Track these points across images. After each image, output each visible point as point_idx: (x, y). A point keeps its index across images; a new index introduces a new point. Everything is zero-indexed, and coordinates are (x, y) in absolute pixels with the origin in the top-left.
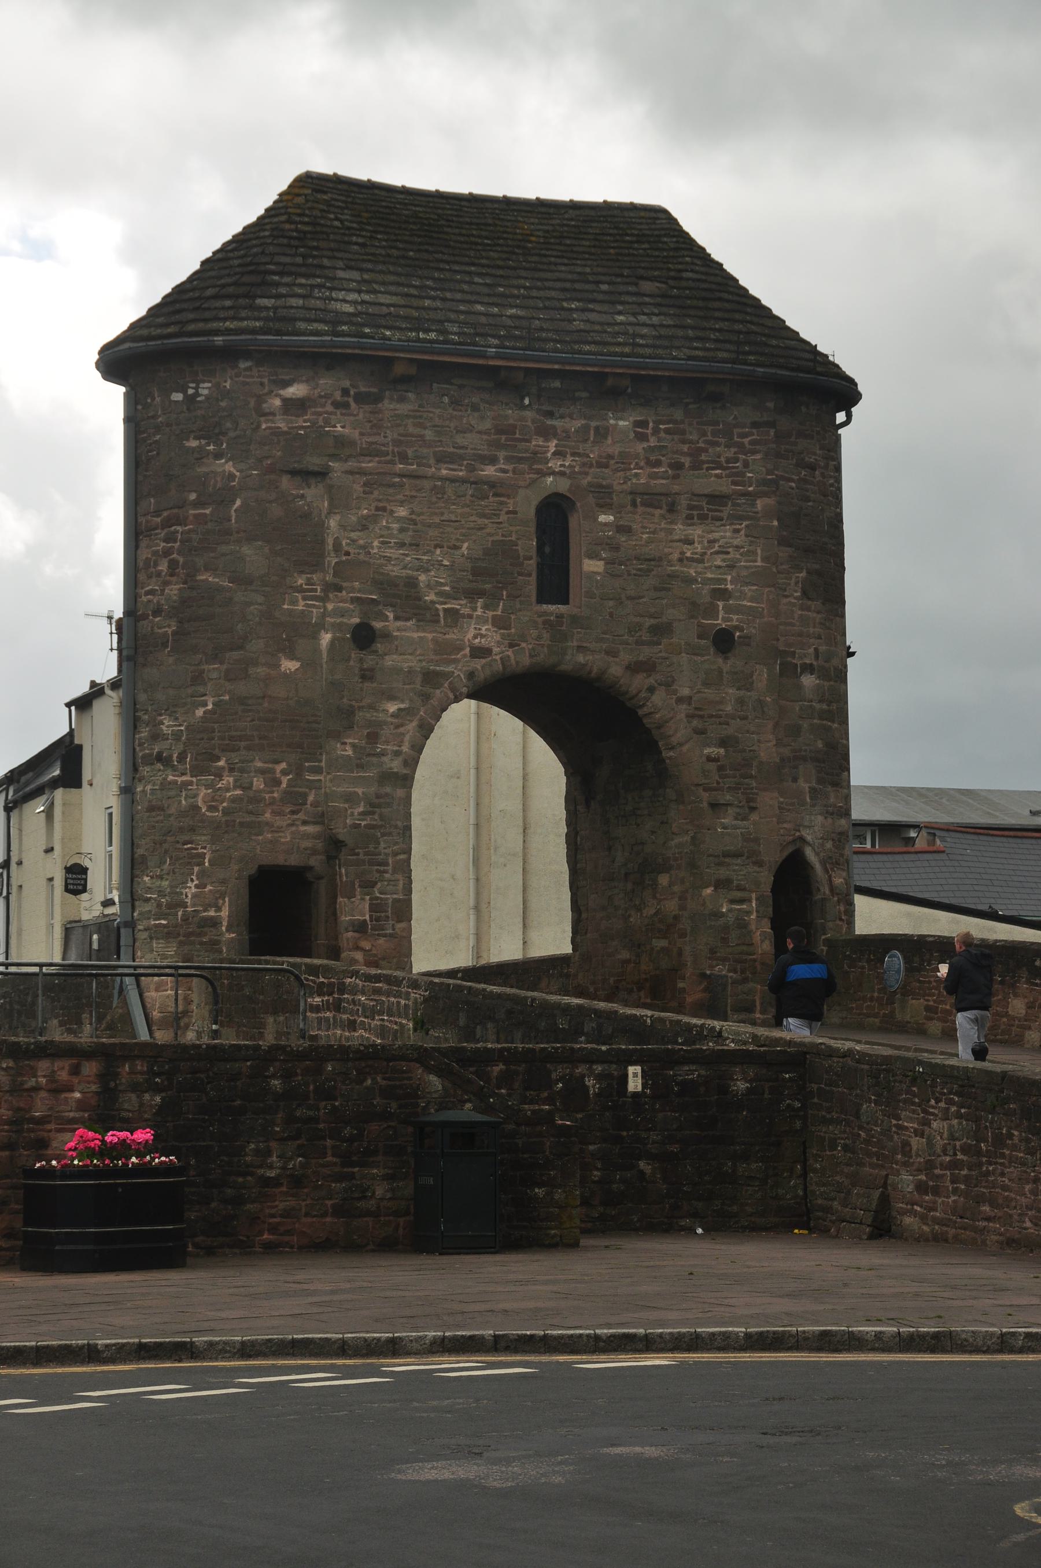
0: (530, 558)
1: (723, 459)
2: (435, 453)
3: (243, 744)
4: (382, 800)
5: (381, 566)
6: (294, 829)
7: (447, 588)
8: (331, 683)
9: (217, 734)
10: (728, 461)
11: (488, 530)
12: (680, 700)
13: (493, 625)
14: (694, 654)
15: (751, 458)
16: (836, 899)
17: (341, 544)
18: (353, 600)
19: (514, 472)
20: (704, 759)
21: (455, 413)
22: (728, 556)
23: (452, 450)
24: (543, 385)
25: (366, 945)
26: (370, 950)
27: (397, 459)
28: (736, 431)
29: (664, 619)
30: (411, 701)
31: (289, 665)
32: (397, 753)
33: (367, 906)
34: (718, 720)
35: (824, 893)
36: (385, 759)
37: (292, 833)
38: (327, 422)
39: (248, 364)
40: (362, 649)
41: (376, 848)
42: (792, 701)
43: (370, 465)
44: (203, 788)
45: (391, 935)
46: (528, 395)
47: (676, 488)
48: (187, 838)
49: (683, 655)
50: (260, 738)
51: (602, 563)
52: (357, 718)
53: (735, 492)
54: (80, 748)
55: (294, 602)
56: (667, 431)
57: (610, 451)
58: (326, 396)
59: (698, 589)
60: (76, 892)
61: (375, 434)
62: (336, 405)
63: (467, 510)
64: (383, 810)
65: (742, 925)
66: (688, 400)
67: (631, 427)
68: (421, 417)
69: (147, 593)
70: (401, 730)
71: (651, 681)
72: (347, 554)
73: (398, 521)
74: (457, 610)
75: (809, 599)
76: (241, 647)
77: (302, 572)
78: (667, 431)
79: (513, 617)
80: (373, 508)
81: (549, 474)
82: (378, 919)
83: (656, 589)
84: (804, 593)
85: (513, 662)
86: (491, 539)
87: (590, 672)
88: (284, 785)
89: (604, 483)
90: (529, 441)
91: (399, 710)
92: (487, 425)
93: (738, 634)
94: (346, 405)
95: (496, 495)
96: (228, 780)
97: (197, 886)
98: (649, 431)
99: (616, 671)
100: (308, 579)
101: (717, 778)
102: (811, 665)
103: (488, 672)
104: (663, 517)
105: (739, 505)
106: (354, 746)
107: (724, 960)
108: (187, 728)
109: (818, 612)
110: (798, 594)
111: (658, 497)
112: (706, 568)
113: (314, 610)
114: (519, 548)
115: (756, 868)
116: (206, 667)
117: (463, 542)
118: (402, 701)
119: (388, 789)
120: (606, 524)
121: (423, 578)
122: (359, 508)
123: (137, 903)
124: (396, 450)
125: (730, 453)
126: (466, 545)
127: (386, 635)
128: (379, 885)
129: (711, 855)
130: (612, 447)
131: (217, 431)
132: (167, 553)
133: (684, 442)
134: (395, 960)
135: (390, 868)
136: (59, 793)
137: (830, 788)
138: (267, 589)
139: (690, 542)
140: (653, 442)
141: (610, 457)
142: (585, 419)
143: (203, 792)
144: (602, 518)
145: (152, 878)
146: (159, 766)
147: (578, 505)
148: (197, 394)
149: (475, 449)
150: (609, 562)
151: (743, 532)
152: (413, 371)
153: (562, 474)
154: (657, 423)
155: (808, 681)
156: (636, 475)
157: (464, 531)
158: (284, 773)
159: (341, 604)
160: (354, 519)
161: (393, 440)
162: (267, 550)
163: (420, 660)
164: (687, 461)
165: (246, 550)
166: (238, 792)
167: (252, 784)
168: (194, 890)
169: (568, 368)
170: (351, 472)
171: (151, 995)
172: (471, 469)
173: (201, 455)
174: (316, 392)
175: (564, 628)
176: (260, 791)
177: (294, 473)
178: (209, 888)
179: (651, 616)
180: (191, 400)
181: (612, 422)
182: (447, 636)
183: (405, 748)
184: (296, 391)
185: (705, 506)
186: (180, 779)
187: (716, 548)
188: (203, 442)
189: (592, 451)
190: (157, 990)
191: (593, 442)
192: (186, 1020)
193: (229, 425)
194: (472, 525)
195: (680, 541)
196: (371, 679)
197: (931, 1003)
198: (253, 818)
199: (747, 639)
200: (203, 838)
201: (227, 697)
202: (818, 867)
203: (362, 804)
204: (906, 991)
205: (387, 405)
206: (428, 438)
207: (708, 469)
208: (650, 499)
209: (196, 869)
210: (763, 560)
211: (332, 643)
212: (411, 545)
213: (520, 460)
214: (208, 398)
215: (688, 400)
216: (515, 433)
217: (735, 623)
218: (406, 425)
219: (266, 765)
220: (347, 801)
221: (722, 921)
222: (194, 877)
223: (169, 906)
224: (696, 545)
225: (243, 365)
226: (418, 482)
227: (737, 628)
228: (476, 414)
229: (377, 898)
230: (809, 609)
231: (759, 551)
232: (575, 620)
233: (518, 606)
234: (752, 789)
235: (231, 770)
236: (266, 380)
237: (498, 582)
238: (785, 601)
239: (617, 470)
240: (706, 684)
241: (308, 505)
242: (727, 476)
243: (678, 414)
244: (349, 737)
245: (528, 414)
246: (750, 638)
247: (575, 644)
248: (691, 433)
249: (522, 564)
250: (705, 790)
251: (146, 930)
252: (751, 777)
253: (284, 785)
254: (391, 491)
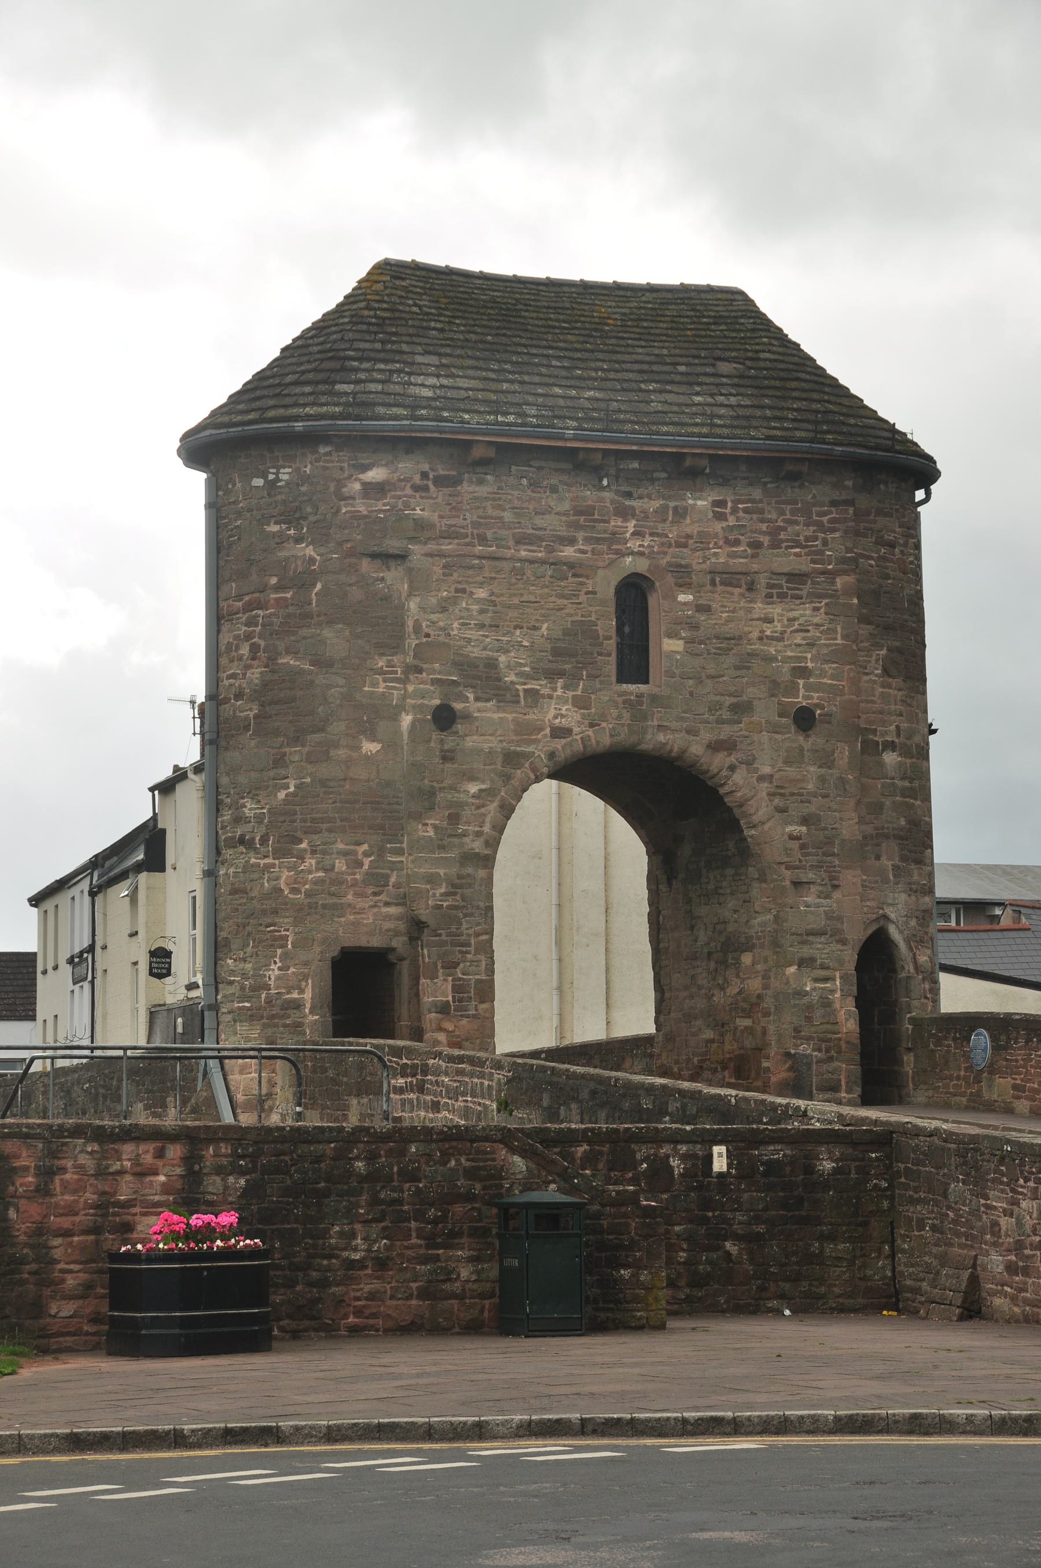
0: (610, 638)
1: (802, 538)
2: (514, 535)
3: (324, 826)
4: (464, 881)
5: (461, 647)
6: (376, 910)
7: (527, 669)
8: (413, 764)
9: (299, 816)
10: (807, 539)
11: (567, 611)
12: (761, 779)
13: (574, 705)
14: (776, 732)
15: (830, 536)
16: (920, 977)
17: (421, 626)
18: (434, 682)
19: (593, 552)
20: (786, 837)
21: (534, 495)
22: (809, 635)
23: (530, 531)
24: (621, 467)
25: (450, 1026)
26: (454, 1031)
27: (476, 541)
28: (814, 509)
29: (745, 698)
30: (492, 781)
31: (370, 747)
32: (478, 834)
33: (450, 988)
34: (799, 798)
35: (909, 972)
36: (467, 840)
37: (375, 914)
38: (407, 506)
39: (328, 449)
40: (442, 730)
41: (458, 929)
42: (874, 779)
43: (450, 547)
44: (285, 870)
45: (474, 1016)
46: (607, 476)
47: (755, 567)
48: (269, 920)
49: (764, 733)
50: (342, 820)
51: (681, 642)
52: (438, 799)
53: (815, 571)
54: (163, 832)
55: (374, 684)
56: (746, 511)
57: (688, 530)
58: (407, 480)
59: (778, 667)
60: (160, 976)
61: (454, 517)
62: (416, 488)
63: (546, 590)
64: (465, 891)
65: (826, 1004)
66: (766, 480)
67: (709, 506)
68: (499, 499)
69: (229, 677)
70: (483, 810)
71: (732, 759)
72: (428, 635)
73: (478, 603)
74: (537, 690)
75: (890, 676)
76: (322, 730)
77: (383, 654)
78: (746, 511)
79: (593, 697)
80: (452, 590)
81: (628, 555)
82: (460, 1000)
83: (737, 668)
84: (885, 670)
85: (594, 741)
86: (570, 619)
87: (671, 751)
88: (366, 867)
89: (683, 563)
90: (607, 522)
91: (481, 790)
92: (566, 506)
93: (818, 712)
94: (426, 489)
95: (575, 575)
96: (311, 862)
97: (280, 969)
98: (729, 510)
99: (696, 749)
100: (389, 661)
101: (800, 856)
102: (893, 742)
103: (568, 752)
104: (743, 595)
105: (818, 583)
106: (435, 827)
107: (809, 1039)
108: (269, 811)
109: (899, 690)
110: (879, 672)
111: (738, 576)
112: (786, 646)
113: (395, 692)
114: (598, 628)
115: (839, 946)
116: (287, 750)
117: (543, 622)
118: (483, 782)
119: (470, 870)
120: (685, 604)
121: (503, 659)
122: (439, 590)
123: (220, 986)
124: (475, 532)
125: (810, 531)
126: (545, 626)
127: (467, 717)
128: (462, 965)
129: (793, 934)
130: (690, 527)
131: (297, 515)
132: (248, 637)
133: (762, 521)
134: (478, 1041)
135: (472, 949)
136: (143, 877)
137: (913, 866)
138: (349, 671)
139: (769, 620)
140: (732, 521)
141: (689, 536)
142: (664, 499)
143: (285, 874)
144: (682, 598)
145: (235, 960)
146: (243, 849)
147: (657, 584)
148: (278, 480)
149: (554, 530)
150: (689, 641)
151: (822, 610)
152: (491, 453)
153: (641, 554)
154: (736, 502)
155: (890, 758)
156: (715, 554)
157: (543, 612)
158: (366, 854)
159: (422, 686)
160: (434, 601)
161: (472, 522)
162: (347, 633)
163: (501, 741)
164: (766, 540)
165: (327, 633)
166: (321, 874)
167: (334, 866)
168: (277, 972)
169: (646, 449)
170: (430, 555)
171: (234, 1078)
172: (551, 550)
173: (281, 539)
174: (395, 475)
175: (644, 707)
176: (342, 873)
177: (374, 556)
178: (292, 970)
179: (731, 695)
180: (271, 485)
181: (690, 502)
182: (527, 717)
183: (487, 829)
184: (375, 474)
185: (785, 584)
186: (262, 862)
187: (796, 627)
188: (284, 526)
189: (670, 531)
190: (241, 1073)
191: (672, 522)
192: (270, 1103)
193: (309, 509)
194: (552, 605)
195: (758, 619)
196: (452, 759)
197: (1019, 1082)
198: (335, 900)
199: (827, 717)
200: (286, 920)
201: (308, 780)
202: (902, 946)
203: (444, 885)
204: (992, 1069)
205: (468, 489)
206: (506, 520)
207: (787, 548)
208: (729, 578)
209: (279, 951)
210: (844, 637)
211: (413, 724)
212: (491, 626)
213: (598, 541)
214: (288, 483)
215: (766, 480)
216: (594, 515)
217: (816, 701)
218: (485, 508)
219: (348, 847)
220: (429, 882)
221: (805, 1000)
222: (277, 960)
223: (253, 989)
224: (776, 623)
225: (323, 449)
226: (497, 563)
227: (817, 705)
228: (555, 496)
229: (460, 979)
230: (890, 687)
231: (839, 629)
232: (654, 699)
233: (598, 686)
234: (835, 867)
235: (314, 852)
236: (346, 465)
237: (578, 663)
238: (866, 678)
239: (695, 550)
240: (787, 762)
241: (388, 588)
242: (806, 554)
243: (757, 493)
244: (429, 818)
245: (607, 494)
246: (831, 715)
247: (656, 723)
248: (769, 512)
249: (602, 643)
250: (787, 868)
251: (229, 1012)
252: (833, 855)
253: (366, 867)
254: (470, 572)
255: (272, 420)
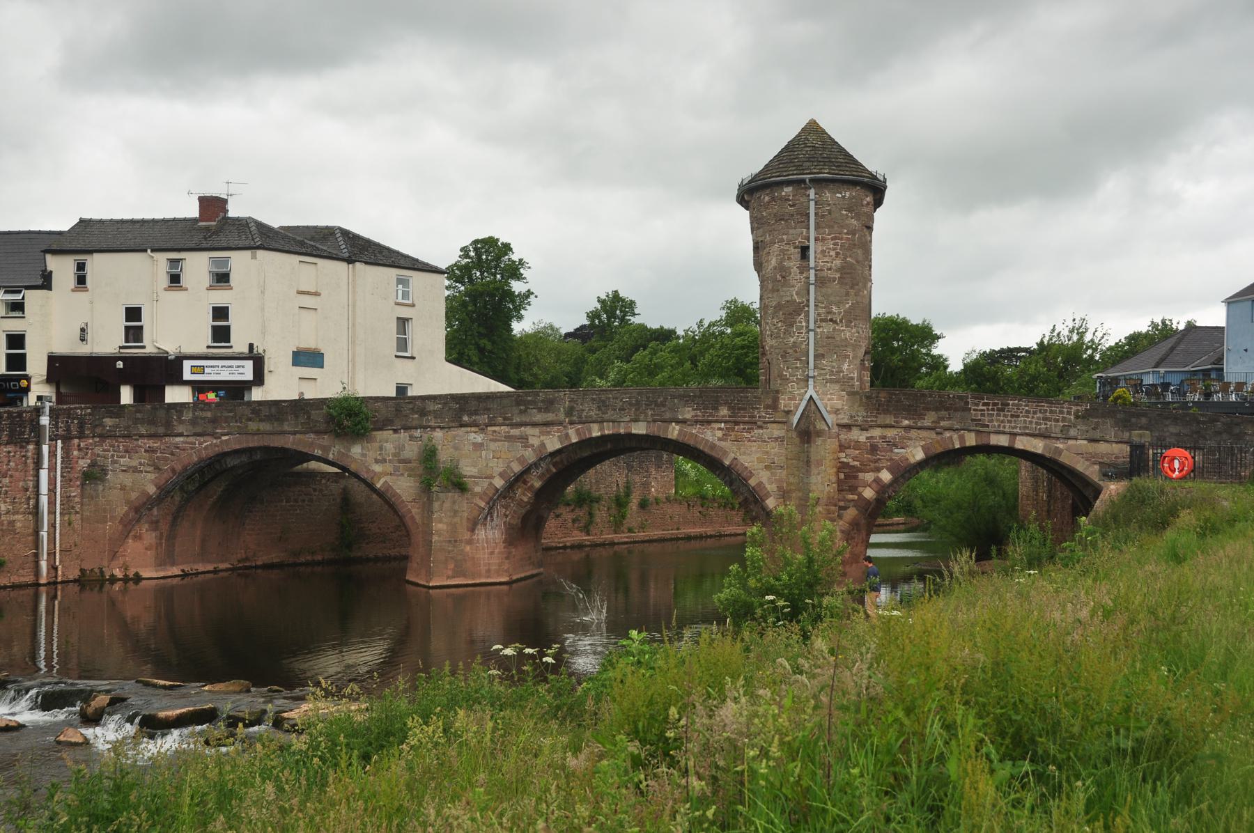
54: (51, 272)
180: (843, 197)
225: (858, 188)
255: (854, 176)
